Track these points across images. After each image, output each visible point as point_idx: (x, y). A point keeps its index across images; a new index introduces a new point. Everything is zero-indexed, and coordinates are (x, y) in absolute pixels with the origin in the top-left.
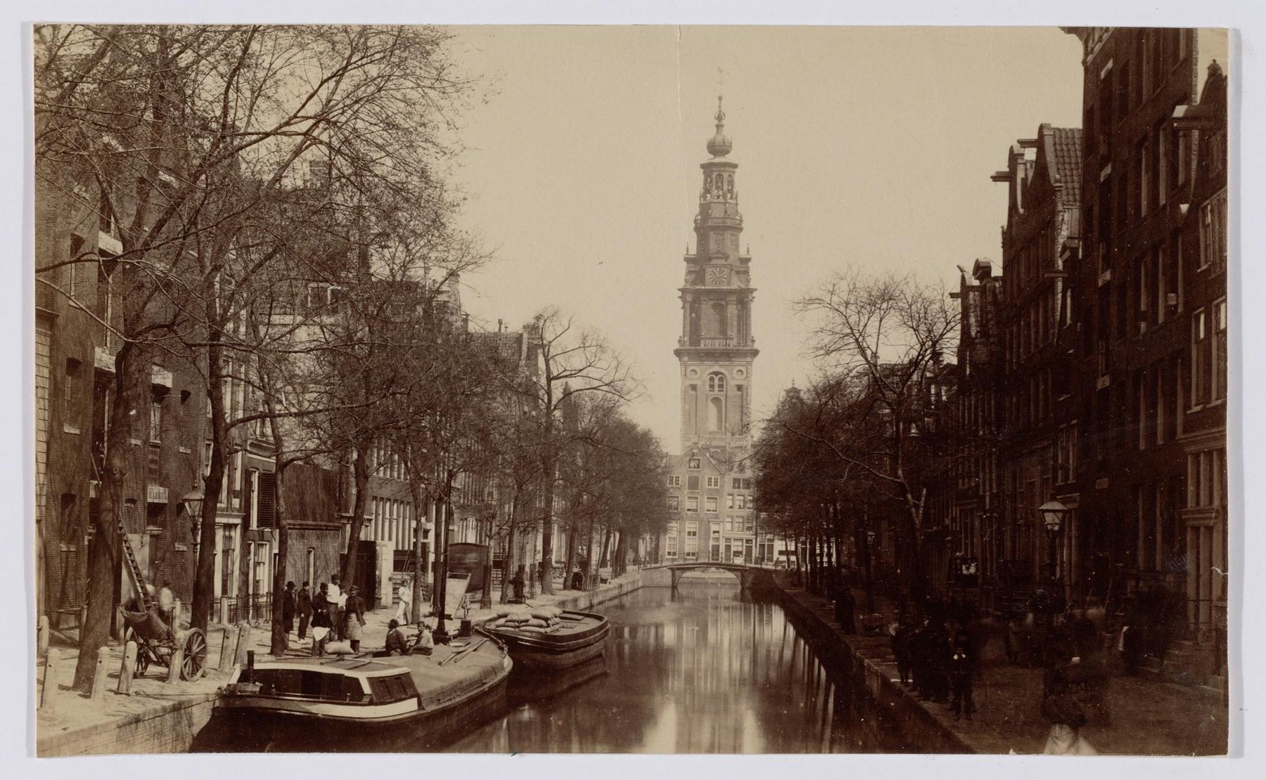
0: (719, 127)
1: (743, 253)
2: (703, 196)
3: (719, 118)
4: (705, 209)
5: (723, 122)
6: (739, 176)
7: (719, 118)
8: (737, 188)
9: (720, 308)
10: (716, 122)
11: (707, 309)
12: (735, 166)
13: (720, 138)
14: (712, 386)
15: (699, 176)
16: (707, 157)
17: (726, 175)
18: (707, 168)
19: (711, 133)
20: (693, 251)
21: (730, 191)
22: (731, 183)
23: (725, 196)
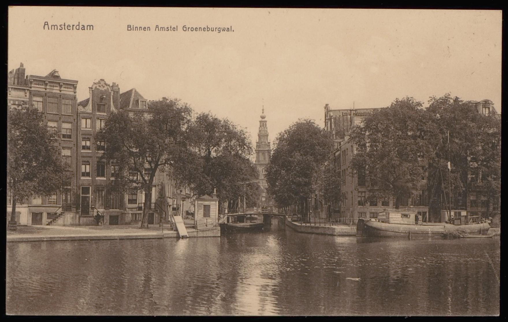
0: (263, 112)
1: (269, 141)
2: (260, 128)
3: (263, 110)
4: (260, 131)
5: (264, 111)
6: (267, 123)
7: (263, 110)
8: (267, 126)
9: (263, 154)
10: (262, 111)
11: (260, 154)
12: (266, 121)
13: (263, 115)
14: (263, 172)
15: (258, 124)
16: (261, 119)
17: (264, 123)
18: (260, 121)
19: (261, 114)
20: (258, 141)
21: (266, 127)
22: (266, 125)
23: (264, 128)
